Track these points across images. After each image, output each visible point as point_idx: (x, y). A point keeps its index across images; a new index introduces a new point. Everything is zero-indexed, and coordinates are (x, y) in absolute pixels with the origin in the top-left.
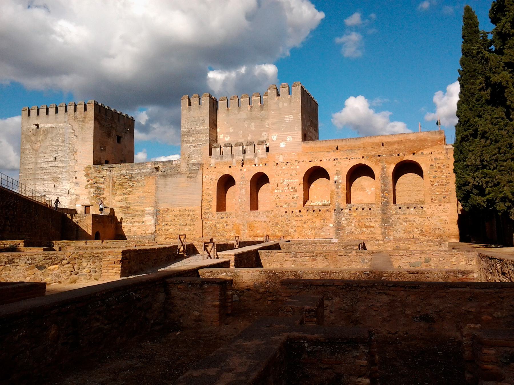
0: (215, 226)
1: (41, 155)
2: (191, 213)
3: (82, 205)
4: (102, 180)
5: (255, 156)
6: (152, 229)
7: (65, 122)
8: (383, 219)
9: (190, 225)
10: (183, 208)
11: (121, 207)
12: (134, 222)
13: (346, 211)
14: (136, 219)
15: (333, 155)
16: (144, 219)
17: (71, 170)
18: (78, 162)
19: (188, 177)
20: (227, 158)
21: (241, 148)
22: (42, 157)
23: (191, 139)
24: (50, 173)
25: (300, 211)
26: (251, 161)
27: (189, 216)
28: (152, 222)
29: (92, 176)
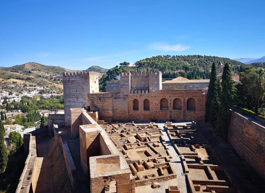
0: (132, 115)
1: (71, 89)
2: (125, 111)
3: (87, 106)
4: (94, 98)
5: (145, 94)
6: (112, 115)
7: (79, 79)
8: (184, 115)
9: (124, 114)
10: (122, 109)
11: (101, 107)
12: (106, 112)
13: (173, 112)
14: (106, 112)
15: (169, 95)
16: (109, 112)
17: (82, 95)
18: (85, 92)
19: (123, 99)
20: (136, 94)
21: (140, 91)
22: (72, 90)
23: (124, 87)
24: (75, 96)
25: (159, 111)
26: (144, 95)
27: (124, 111)
28: (112, 113)
29: (90, 97)
